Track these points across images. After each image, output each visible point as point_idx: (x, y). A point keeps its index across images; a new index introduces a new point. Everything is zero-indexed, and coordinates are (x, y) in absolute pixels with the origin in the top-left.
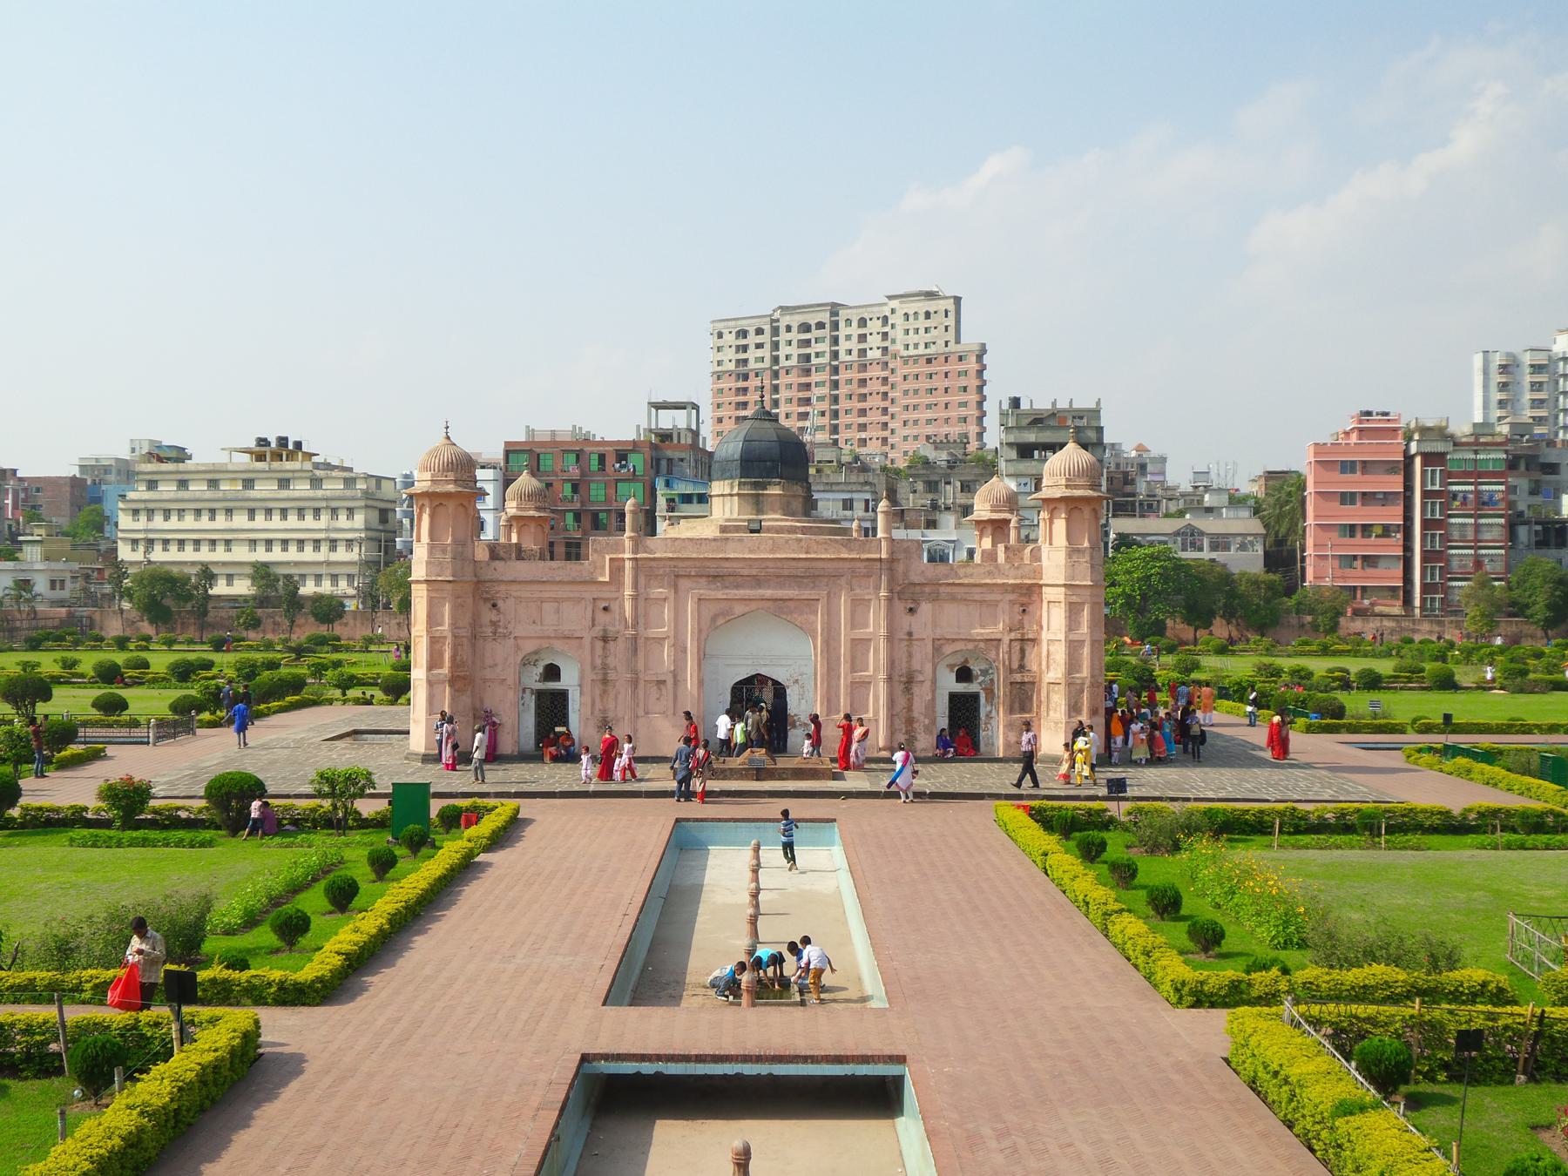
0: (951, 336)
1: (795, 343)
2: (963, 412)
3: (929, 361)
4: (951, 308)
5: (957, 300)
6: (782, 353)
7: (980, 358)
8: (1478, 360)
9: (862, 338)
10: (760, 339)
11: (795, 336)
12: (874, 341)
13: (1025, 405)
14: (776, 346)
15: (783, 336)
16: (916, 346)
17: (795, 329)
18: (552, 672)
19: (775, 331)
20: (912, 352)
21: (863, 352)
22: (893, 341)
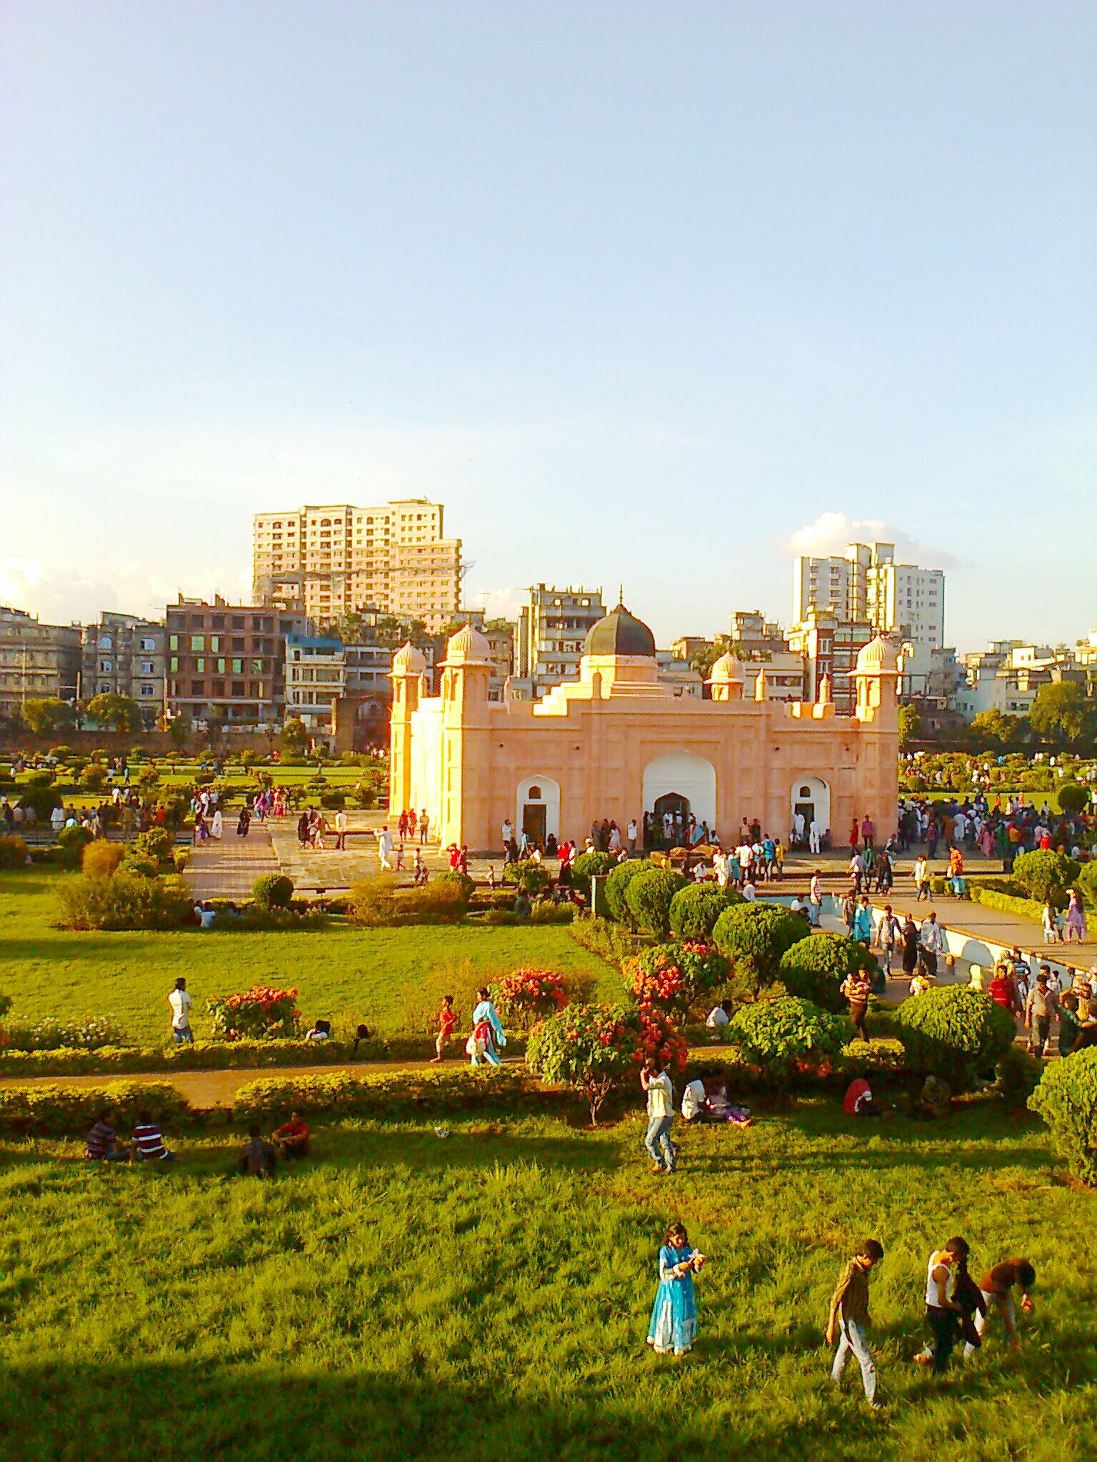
0: (437, 533)
1: (318, 534)
2: (444, 588)
3: (420, 551)
4: (438, 513)
5: (441, 507)
6: (308, 541)
7: (457, 549)
8: (798, 563)
9: (370, 532)
10: (291, 530)
11: (318, 528)
12: (379, 534)
13: (548, 588)
14: (304, 534)
15: (309, 529)
16: (410, 540)
17: (318, 523)
18: (535, 793)
19: (303, 524)
20: (407, 543)
21: (370, 542)
22: (393, 535)
